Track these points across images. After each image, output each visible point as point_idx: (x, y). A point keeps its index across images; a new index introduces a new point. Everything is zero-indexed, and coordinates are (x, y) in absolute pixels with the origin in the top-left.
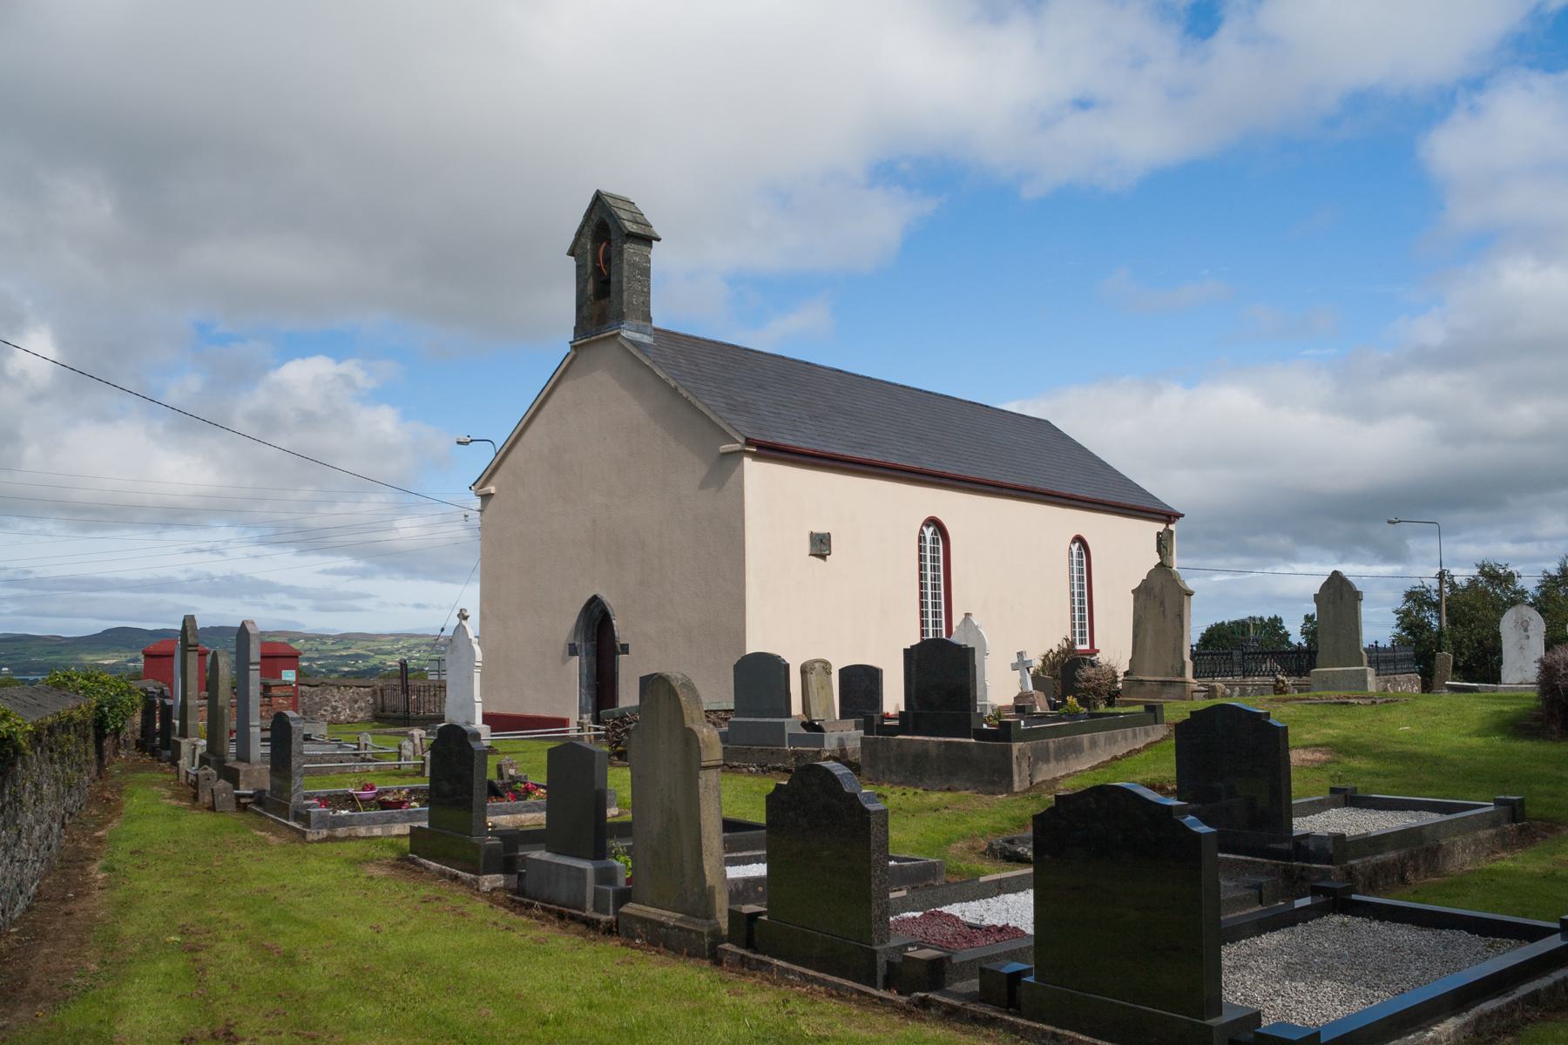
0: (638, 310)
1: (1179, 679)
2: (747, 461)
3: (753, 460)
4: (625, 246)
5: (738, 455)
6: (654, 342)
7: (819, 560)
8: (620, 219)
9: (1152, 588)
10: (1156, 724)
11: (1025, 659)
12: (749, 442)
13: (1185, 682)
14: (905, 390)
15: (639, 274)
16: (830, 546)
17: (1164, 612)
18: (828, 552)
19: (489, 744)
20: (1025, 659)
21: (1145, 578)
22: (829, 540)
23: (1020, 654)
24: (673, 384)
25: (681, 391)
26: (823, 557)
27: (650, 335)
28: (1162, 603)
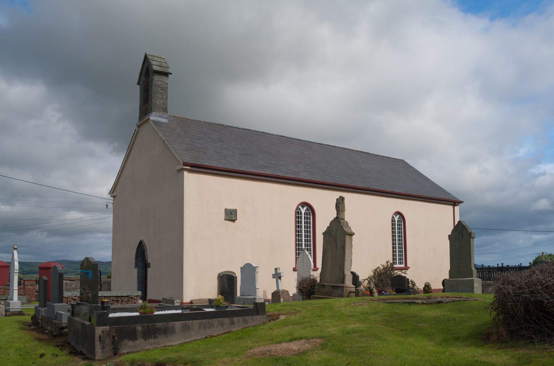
0: (160, 107)
1: (341, 285)
2: (186, 173)
3: (188, 173)
4: (153, 77)
5: (181, 170)
6: (169, 122)
7: (230, 222)
8: (151, 65)
9: (332, 232)
10: (258, 315)
11: (278, 272)
12: (185, 164)
13: (343, 287)
14: (238, 129)
15: (161, 90)
16: (236, 216)
17: (336, 245)
18: (235, 219)
19: (21, 310)
20: (278, 272)
21: (329, 226)
22: (236, 213)
23: (276, 269)
24: (163, 138)
25: (166, 142)
26: (234, 221)
27: (167, 118)
28: (336, 240)
